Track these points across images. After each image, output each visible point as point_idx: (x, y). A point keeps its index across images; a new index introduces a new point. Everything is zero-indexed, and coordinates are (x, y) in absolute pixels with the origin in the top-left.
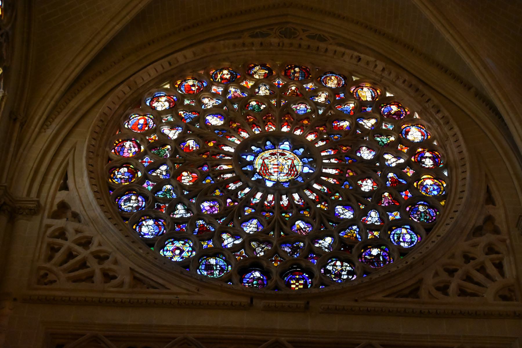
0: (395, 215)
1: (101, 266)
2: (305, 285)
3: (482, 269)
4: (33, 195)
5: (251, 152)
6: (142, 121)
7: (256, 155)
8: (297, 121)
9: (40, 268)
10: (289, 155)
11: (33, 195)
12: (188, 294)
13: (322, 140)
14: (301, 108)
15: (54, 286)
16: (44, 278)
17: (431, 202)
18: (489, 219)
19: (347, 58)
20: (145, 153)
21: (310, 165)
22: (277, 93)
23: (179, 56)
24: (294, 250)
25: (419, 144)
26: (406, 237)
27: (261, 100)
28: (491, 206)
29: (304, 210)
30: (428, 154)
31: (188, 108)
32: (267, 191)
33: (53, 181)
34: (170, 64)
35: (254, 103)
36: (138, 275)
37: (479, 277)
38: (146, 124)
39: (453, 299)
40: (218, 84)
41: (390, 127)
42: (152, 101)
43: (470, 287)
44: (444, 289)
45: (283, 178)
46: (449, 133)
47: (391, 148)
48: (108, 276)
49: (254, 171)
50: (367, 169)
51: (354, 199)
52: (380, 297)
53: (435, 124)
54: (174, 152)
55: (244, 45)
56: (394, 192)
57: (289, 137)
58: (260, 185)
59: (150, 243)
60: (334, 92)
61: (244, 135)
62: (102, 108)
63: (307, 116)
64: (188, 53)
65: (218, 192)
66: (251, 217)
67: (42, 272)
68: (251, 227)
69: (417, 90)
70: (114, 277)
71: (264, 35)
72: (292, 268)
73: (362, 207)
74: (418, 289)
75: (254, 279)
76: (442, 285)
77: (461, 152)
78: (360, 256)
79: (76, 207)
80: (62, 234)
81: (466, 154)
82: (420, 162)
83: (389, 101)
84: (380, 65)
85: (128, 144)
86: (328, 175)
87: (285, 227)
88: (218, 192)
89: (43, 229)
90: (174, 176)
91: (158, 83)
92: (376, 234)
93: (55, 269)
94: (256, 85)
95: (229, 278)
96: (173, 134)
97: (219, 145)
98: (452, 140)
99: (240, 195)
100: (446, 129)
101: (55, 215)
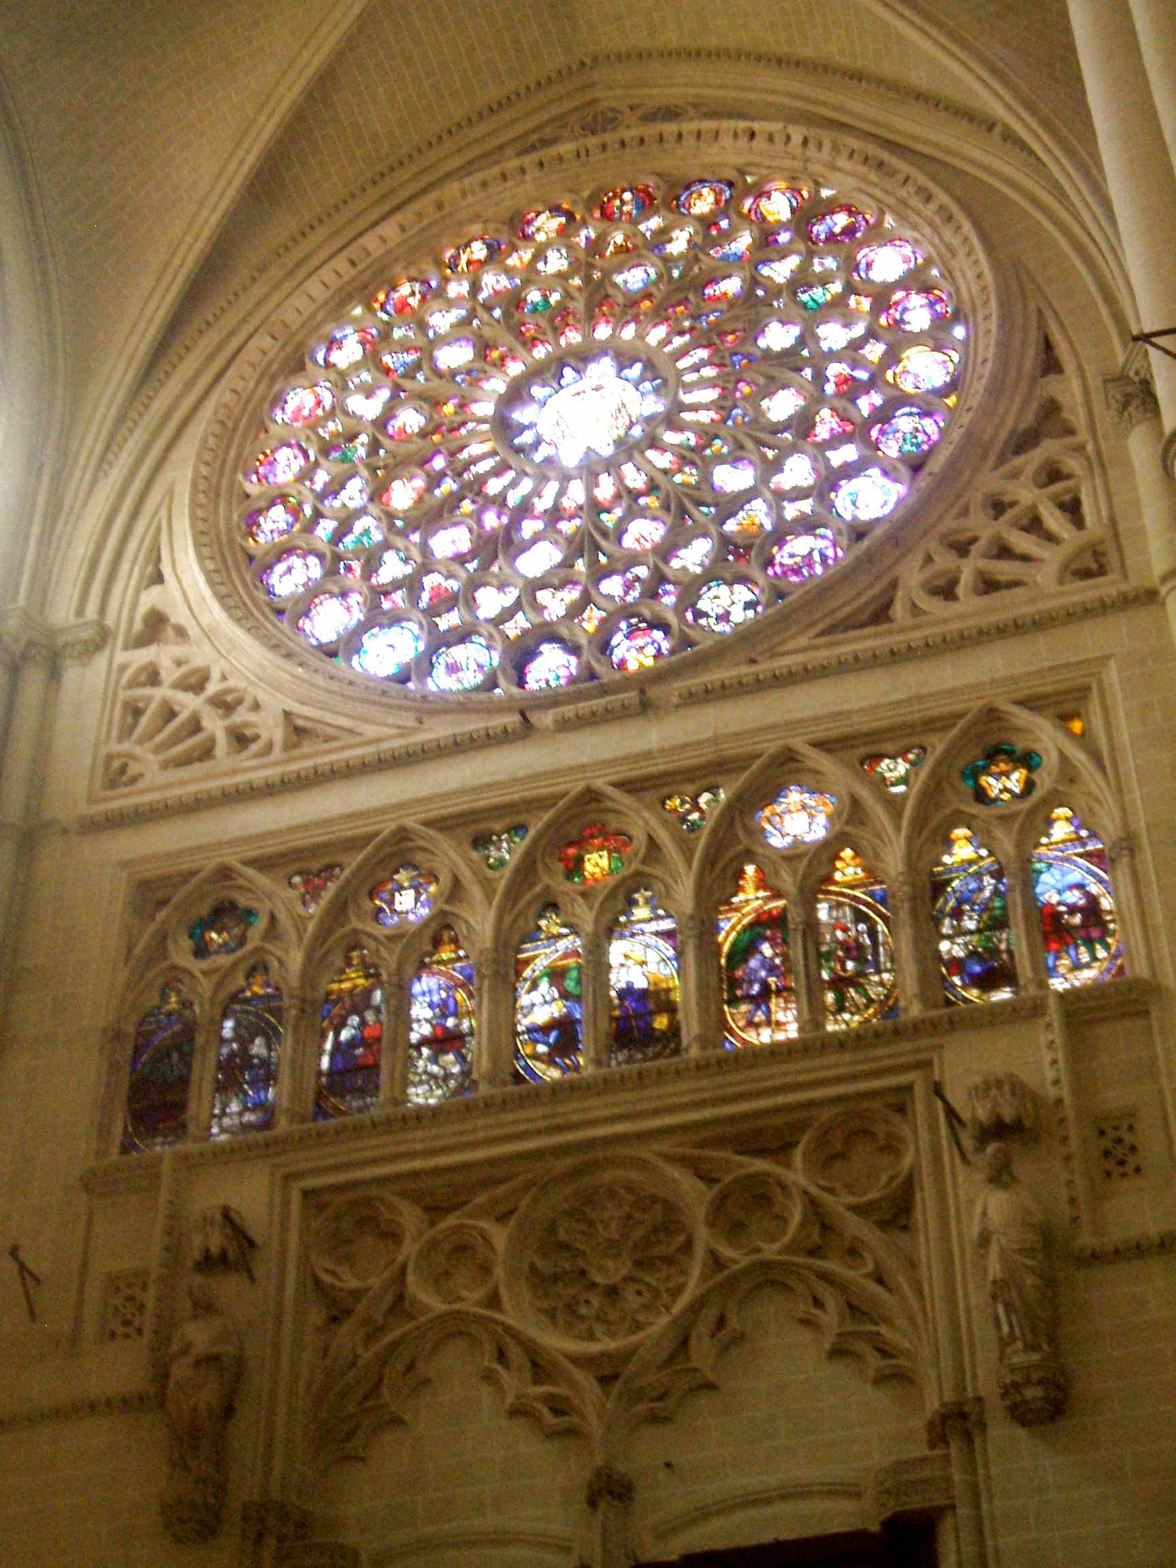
0: (847, 453)
1: (228, 722)
4: (91, 612)
8: (630, 308)
9: (110, 758)
11: (91, 612)
12: (402, 736)
13: (681, 333)
14: (634, 279)
15: (140, 785)
16: (118, 775)
18: (1051, 409)
19: (727, 141)
20: (317, 465)
22: (586, 261)
23: (370, 241)
26: (872, 497)
28: (1052, 377)
29: (647, 493)
32: (565, 478)
33: (131, 571)
34: (353, 263)
36: (300, 722)
37: (1023, 542)
38: (319, 403)
39: (969, 608)
40: (460, 277)
41: (830, 263)
42: (329, 350)
43: (1005, 569)
44: (947, 591)
46: (955, 241)
48: (241, 739)
52: (803, 641)
53: (927, 230)
54: (374, 447)
55: (504, 177)
56: (841, 404)
59: (330, 652)
60: (707, 222)
62: (223, 394)
64: (389, 230)
65: (467, 506)
66: (536, 538)
67: (116, 764)
68: (539, 560)
69: (881, 164)
70: (256, 738)
71: (546, 143)
73: (770, 454)
74: (889, 604)
76: (942, 582)
77: (979, 276)
78: (770, 562)
79: (178, 615)
80: (152, 677)
81: (989, 276)
83: (831, 208)
84: (797, 133)
85: (284, 454)
86: (694, 408)
87: (603, 543)
89: (114, 676)
91: (337, 308)
92: (806, 506)
93: (138, 750)
94: (540, 255)
97: (462, 406)
98: (962, 252)
99: (513, 499)
100: (948, 234)
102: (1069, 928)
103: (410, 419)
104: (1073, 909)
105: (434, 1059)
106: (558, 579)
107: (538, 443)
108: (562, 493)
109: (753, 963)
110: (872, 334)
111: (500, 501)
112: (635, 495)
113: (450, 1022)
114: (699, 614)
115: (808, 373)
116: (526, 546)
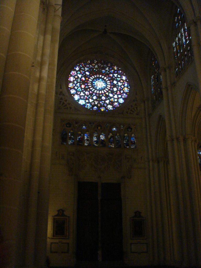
2: (104, 110)
3: (134, 109)
5: (94, 81)
6: (74, 73)
7: (95, 82)
10: (101, 82)
17: (126, 93)
21: (105, 84)
24: (102, 103)
25: (125, 81)
26: (121, 101)
27: (96, 69)
30: (126, 83)
31: (82, 70)
35: (95, 69)
38: (75, 73)
45: (100, 87)
47: (119, 81)
48: (71, 108)
49: (95, 86)
50: (115, 86)
51: (112, 92)
57: (101, 78)
58: (96, 89)
61: (93, 77)
63: (105, 73)
65: (88, 90)
72: (101, 106)
75: (95, 108)
80: (61, 99)
82: (124, 84)
83: (120, 70)
88: (88, 90)
90: (81, 86)
94: (95, 65)
95: (91, 108)
96: (80, 76)
99: (92, 90)
101: (60, 95)
102: (133, 143)
103: (83, 79)
104: (133, 141)
105: (87, 141)
106: (96, 100)
107: (95, 86)
108: (97, 91)
109: (111, 140)
110: (123, 85)
111: (91, 90)
112: (103, 94)
113: (88, 139)
114: (108, 107)
115: (117, 87)
116: (94, 96)
